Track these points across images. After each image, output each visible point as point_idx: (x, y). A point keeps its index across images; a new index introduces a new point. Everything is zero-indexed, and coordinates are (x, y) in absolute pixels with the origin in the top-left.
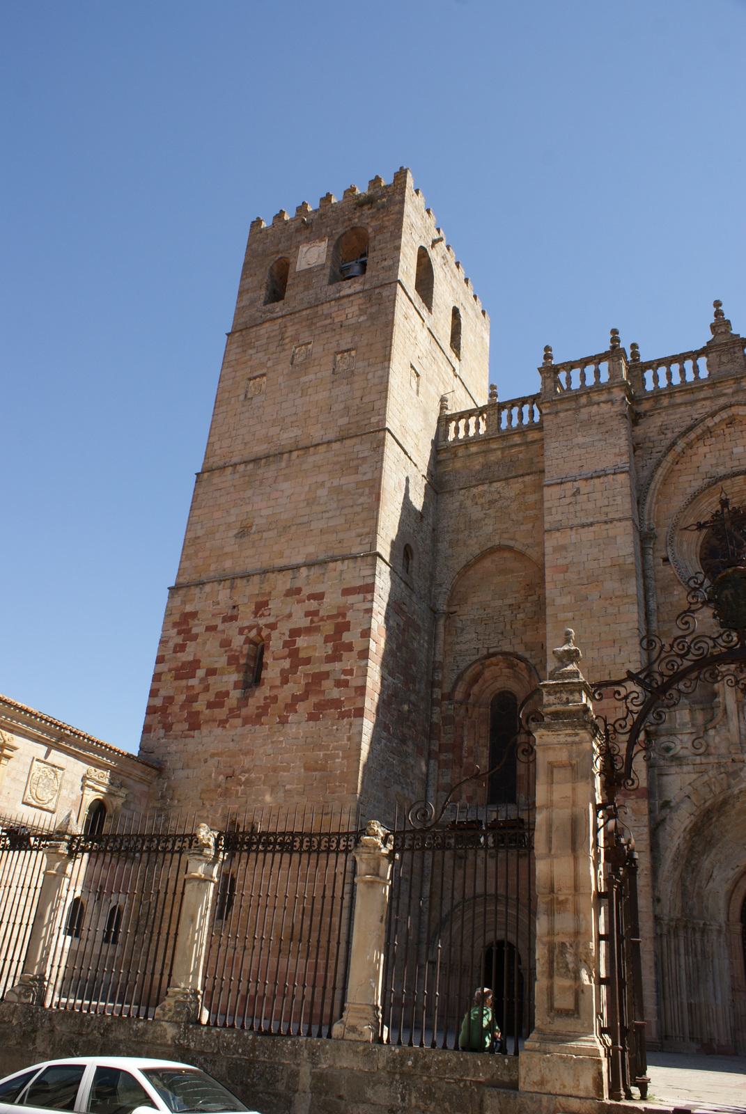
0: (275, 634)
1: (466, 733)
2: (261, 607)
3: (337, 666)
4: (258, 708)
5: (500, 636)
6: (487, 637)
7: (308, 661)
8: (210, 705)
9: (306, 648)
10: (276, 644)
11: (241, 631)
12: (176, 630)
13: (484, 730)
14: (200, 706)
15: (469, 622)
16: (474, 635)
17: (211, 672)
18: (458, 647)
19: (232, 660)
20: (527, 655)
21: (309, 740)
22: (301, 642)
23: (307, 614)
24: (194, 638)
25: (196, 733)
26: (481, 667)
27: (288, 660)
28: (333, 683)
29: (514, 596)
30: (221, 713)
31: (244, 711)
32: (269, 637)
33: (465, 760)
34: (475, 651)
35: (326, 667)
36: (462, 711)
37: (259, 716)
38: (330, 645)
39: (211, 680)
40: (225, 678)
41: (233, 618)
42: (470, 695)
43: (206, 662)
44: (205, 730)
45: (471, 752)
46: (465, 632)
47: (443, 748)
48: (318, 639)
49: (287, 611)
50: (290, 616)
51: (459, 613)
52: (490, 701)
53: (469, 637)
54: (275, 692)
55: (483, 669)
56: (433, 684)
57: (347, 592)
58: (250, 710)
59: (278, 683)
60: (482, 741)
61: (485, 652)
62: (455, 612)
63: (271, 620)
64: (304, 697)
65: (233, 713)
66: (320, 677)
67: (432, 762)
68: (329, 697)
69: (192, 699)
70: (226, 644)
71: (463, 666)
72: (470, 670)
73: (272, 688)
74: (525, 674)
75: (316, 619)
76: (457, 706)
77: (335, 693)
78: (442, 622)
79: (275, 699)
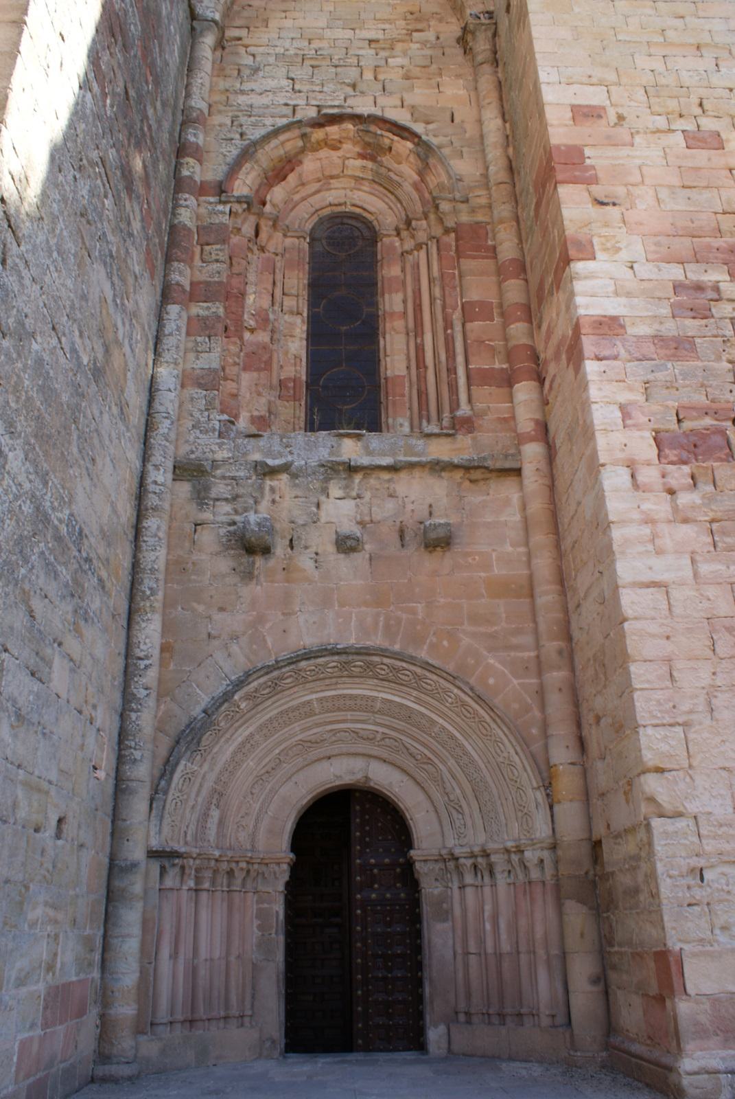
1: (252, 277)
5: (349, 90)
6: (317, 88)
13: (297, 281)
15: (272, 60)
16: (285, 82)
18: (242, 99)
20: (418, 128)
26: (300, 143)
29: (383, 26)
33: (247, 335)
34: (288, 111)
36: (248, 229)
42: (264, 204)
45: (264, 321)
46: (261, 74)
47: (200, 292)
51: (245, 41)
52: (309, 226)
53: (271, 83)
55: (303, 150)
56: (182, 150)
60: (289, 303)
61: (312, 113)
62: (240, 39)
67: (173, 309)
71: (257, 134)
72: (274, 142)
74: (408, 171)
76: (238, 208)
78: (209, 40)
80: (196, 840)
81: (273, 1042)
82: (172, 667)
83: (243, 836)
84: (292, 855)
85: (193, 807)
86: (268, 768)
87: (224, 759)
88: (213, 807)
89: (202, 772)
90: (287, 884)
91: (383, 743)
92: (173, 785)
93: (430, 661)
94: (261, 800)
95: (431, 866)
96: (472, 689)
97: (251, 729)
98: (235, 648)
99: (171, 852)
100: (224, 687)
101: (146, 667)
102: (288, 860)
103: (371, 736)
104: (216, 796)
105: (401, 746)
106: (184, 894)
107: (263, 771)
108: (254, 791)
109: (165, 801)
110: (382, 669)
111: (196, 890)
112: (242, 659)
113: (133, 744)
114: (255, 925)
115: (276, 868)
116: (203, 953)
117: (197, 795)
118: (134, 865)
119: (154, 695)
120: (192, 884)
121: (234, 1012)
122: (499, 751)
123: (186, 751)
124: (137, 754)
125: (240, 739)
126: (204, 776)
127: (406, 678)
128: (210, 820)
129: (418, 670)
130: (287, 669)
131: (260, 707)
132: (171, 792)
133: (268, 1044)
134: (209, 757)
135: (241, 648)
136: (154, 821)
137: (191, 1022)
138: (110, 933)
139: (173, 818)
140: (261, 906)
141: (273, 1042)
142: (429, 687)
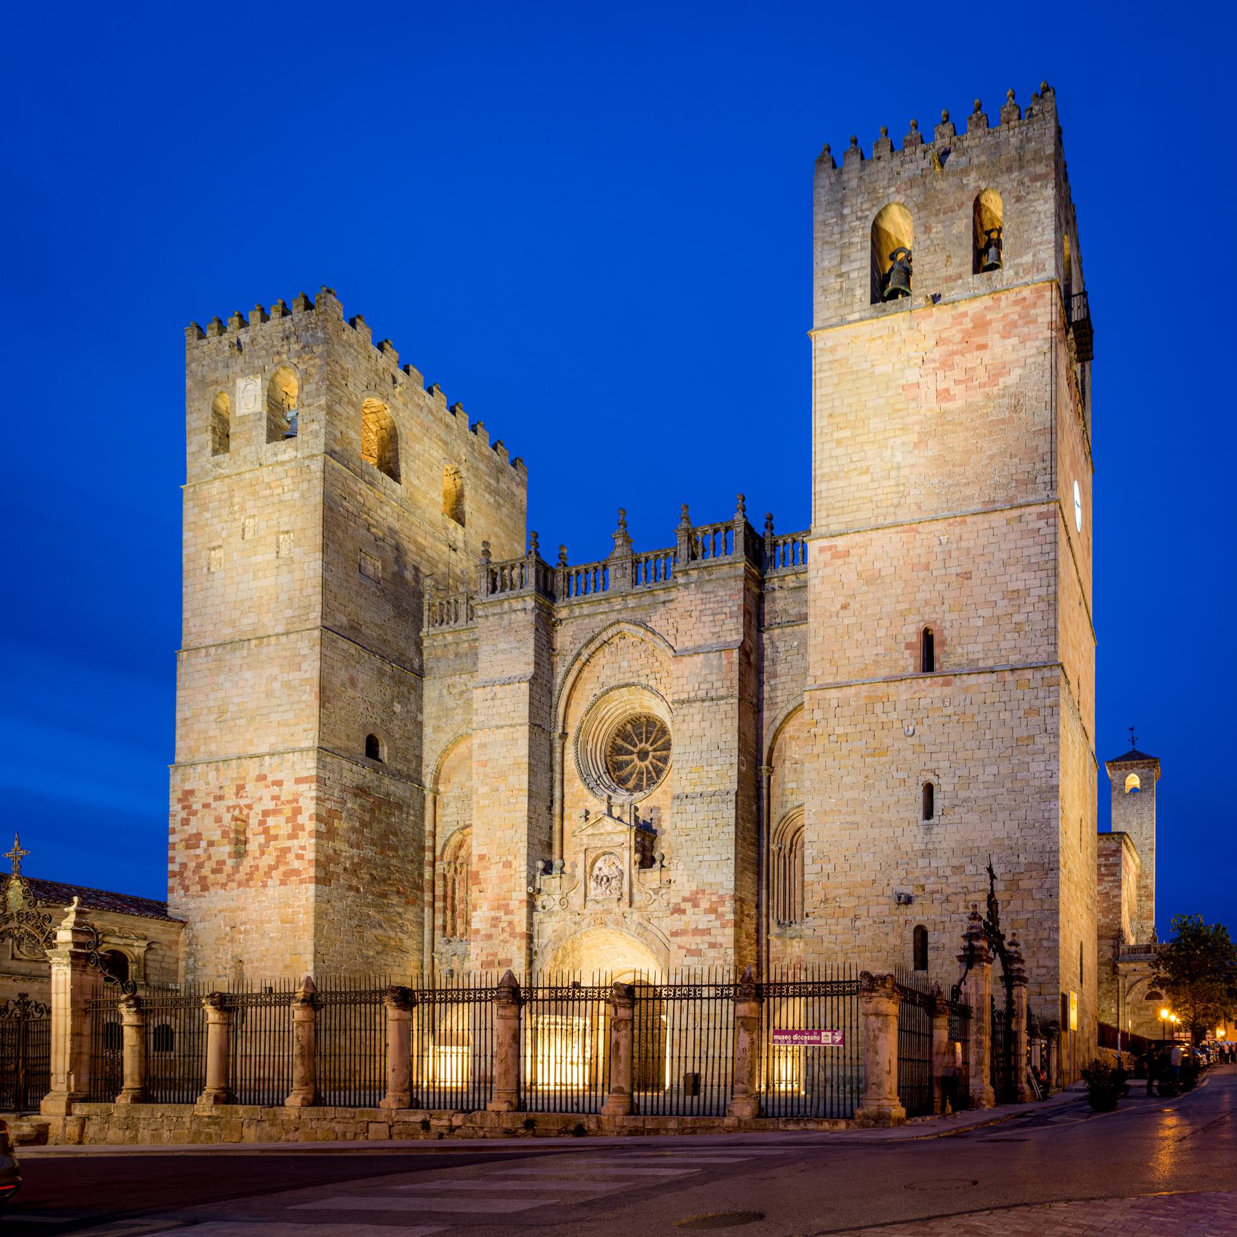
0: (252, 814)
2: (240, 788)
3: (295, 843)
4: (247, 874)
7: (276, 838)
8: (214, 871)
9: (275, 827)
10: (253, 822)
11: (228, 811)
12: (180, 806)
14: (206, 871)
17: (211, 844)
19: (225, 834)
21: (282, 900)
22: (271, 821)
23: (274, 798)
24: (195, 813)
25: (206, 893)
27: (263, 836)
28: (294, 856)
30: (222, 878)
31: (237, 877)
32: (248, 814)
35: (288, 843)
37: (248, 880)
38: (290, 825)
39: (212, 850)
40: (221, 849)
41: (220, 798)
43: (205, 835)
44: (212, 890)
48: (281, 819)
49: (258, 795)
50: (261, 799)
54: (257, 862)
57: (299, 781)
58: (240, 876)
59: (258, 854)
63: (248, 801)
64: (275, 867)
65: (230, 878)
66: (285, 851)
68: (291, 868)
69: (200, 866)
70: (218, 820)
73: (254, 858)
75: (279, 803)
77: (296, 864)
79: (257, 867)
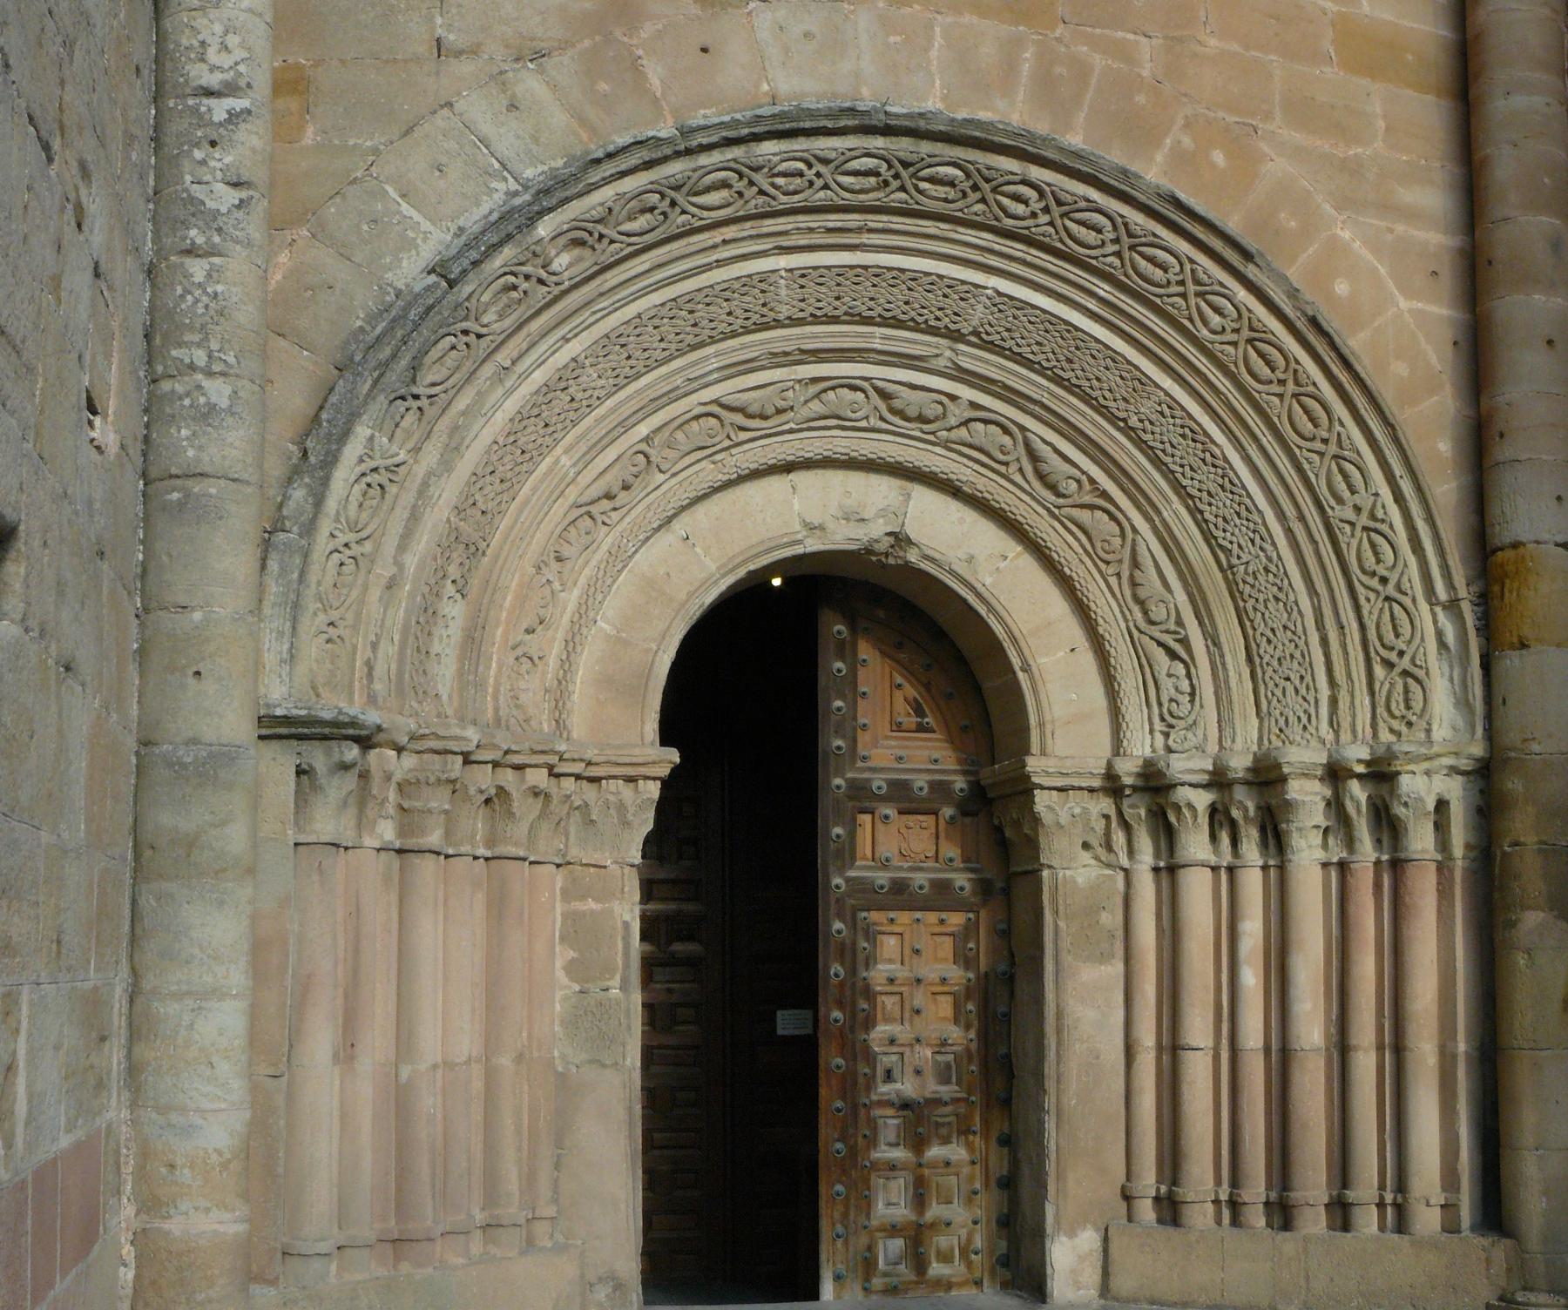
80: (401, 693)
81: (619, 1286)
82: (310, 136)
83: (533, 690)
84: (674, 755)
85: (391, 585)
86: (612, 480)
87: (486, 437)
88: (450, 589)
89: (420, 470)
90: (653, 845)
91: (962, 433)
92: (331, 504)
93: (1182, 196)
94: (582, 581)
95: (1077, 803)
96: (1293, 293)
97: (574, 348)
98: (530, 84)
99: (335, 724)
100: (499, 197)
101: (234, 117)
102: (664, 771)
103: (933, 410)
104: (458, 554)
105: (1021, 449)
106: (371, 868)
107: (595, 491)
108: (566, 551)
109: (306, 556)
110: (1017, 198)
111: (400, 851)
112: (559, 118)
113: (200, 357)
114: (559, 964)
115: (627, 792)
116: (430, 1045)
117: (402, 547)
118: (224, 756)
119: (261, 207)
120: (387, 831)
121: (512, 1210)
122: (1342, 487)
123: (370, 395)
124: (218, 391)
125: (539, 377)
126: (425, 484)
127: (1090, 237)
128: (439, 631)
129: (1137, 218)
130: (716, 157)
131: (613, 278)
132: (325, 526)
133: (602, 1293)
134: (443, 425)
135: (554, 87)
136: (274, 620)
137: (399, 1244)
138: (147, 984)
139: (334, 615)
140: (578, 906)
141: (619, 1286)
142: (1158, 274)
